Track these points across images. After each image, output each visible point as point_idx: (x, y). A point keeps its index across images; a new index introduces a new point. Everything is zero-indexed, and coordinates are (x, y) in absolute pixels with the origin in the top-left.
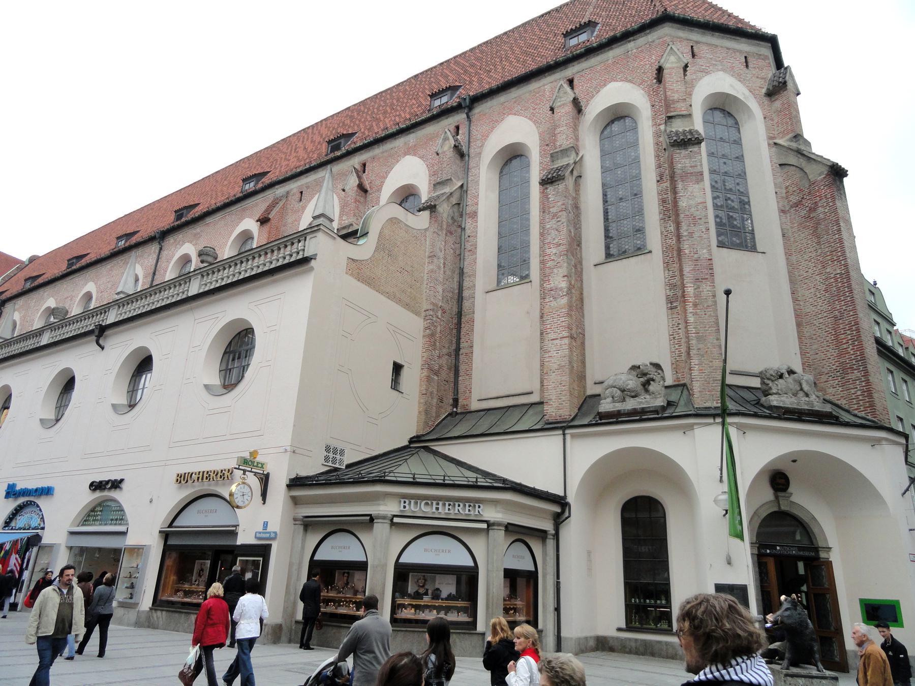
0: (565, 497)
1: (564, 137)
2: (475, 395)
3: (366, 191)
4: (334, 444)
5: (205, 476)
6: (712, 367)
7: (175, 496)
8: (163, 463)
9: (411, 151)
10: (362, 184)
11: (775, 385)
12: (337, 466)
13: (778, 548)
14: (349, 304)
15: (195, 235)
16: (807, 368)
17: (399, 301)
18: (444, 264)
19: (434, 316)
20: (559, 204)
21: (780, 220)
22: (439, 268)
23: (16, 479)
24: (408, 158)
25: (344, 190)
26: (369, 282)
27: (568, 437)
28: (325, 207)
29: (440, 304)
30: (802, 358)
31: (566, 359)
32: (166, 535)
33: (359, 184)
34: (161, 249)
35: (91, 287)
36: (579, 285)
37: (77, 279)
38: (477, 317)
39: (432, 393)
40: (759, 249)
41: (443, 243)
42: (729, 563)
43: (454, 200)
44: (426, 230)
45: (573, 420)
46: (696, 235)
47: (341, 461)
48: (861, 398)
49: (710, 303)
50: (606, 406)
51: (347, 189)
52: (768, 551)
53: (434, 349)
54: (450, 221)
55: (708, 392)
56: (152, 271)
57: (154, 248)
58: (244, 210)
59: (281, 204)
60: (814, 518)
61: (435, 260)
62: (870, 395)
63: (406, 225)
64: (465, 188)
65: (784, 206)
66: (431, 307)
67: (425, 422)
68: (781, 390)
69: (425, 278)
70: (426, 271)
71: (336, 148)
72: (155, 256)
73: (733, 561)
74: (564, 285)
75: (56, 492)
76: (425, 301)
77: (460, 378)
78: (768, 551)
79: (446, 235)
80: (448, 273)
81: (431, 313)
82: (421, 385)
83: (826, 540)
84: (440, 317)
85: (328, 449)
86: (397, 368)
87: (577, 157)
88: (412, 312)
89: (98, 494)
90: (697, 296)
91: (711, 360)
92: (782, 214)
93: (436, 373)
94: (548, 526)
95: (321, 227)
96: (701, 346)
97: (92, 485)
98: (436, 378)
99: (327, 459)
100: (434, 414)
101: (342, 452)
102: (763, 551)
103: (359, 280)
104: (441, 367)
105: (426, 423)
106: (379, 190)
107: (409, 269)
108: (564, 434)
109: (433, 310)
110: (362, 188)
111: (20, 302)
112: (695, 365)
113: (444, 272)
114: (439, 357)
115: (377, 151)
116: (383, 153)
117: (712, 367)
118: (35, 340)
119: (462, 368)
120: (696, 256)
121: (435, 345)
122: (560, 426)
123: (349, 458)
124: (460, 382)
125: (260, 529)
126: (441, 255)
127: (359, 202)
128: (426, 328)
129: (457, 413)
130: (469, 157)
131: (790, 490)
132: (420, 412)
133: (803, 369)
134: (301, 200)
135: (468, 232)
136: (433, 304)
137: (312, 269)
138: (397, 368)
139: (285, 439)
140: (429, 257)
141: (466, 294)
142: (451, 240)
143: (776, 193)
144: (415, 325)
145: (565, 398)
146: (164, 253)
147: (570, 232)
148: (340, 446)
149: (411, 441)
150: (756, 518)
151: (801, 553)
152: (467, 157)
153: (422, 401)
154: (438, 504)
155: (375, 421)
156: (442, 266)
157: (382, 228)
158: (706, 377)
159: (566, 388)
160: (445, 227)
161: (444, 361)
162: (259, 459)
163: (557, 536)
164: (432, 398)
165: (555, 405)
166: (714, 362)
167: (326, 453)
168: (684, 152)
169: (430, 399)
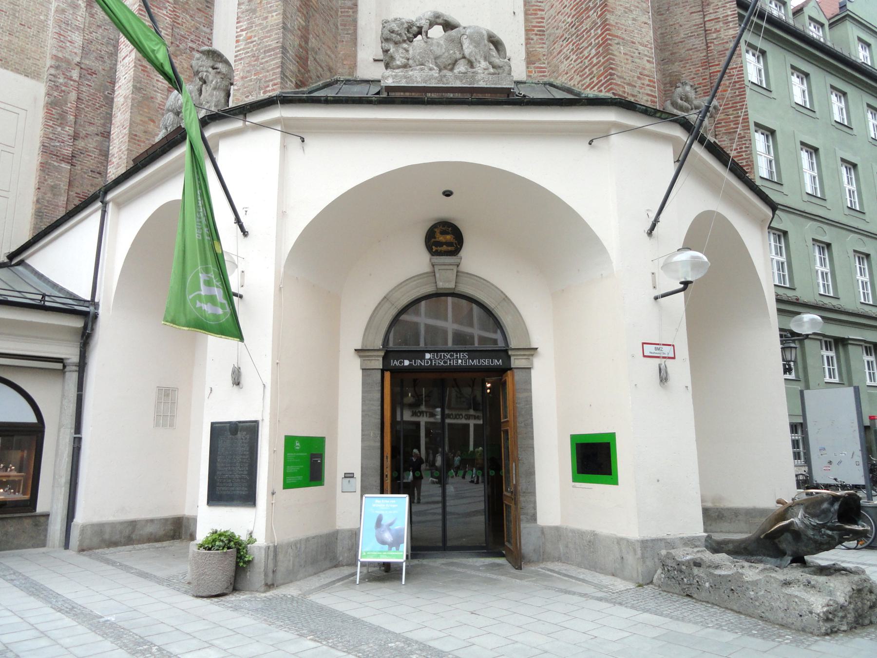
0: (93, 302)
6: (267, 27)
11: (401, 50)
13: (428, 356)
16: (535, 38)
19: (62, 76)
27: (110, 208)
29: (78, 59)
30: (526, 20)
39: (53, 188)
42: (237, 383)
48: (595, 61)
52: (407, 363)
55: (255, 74)
60: (506, 299)
62: (607, 51)
66: (53, 63)
68: (413, 58)
69: (51, 23)
73: (244, 380)
78: (407, 363)
81: (53, 71)
83: (526, 333)
91: (265, 15)
93: (72, 160)
94: (70, 353)
98: (66, 166)
102: (396, 363)
112: (242, 31)
114: (75, 137)
117: (267, 27)
121: (62, 117)
128: (48, 94)
131: (463, 253)
133: (528, 40)
136: (56, 58)
150: (387, 305)
151: (476, 362)
153: (35, 199)
158: (254, 49)
159: (126, 131)
163: (82, 366)
164: (54, 195)
166: (270, 18)
169: (49, 195)
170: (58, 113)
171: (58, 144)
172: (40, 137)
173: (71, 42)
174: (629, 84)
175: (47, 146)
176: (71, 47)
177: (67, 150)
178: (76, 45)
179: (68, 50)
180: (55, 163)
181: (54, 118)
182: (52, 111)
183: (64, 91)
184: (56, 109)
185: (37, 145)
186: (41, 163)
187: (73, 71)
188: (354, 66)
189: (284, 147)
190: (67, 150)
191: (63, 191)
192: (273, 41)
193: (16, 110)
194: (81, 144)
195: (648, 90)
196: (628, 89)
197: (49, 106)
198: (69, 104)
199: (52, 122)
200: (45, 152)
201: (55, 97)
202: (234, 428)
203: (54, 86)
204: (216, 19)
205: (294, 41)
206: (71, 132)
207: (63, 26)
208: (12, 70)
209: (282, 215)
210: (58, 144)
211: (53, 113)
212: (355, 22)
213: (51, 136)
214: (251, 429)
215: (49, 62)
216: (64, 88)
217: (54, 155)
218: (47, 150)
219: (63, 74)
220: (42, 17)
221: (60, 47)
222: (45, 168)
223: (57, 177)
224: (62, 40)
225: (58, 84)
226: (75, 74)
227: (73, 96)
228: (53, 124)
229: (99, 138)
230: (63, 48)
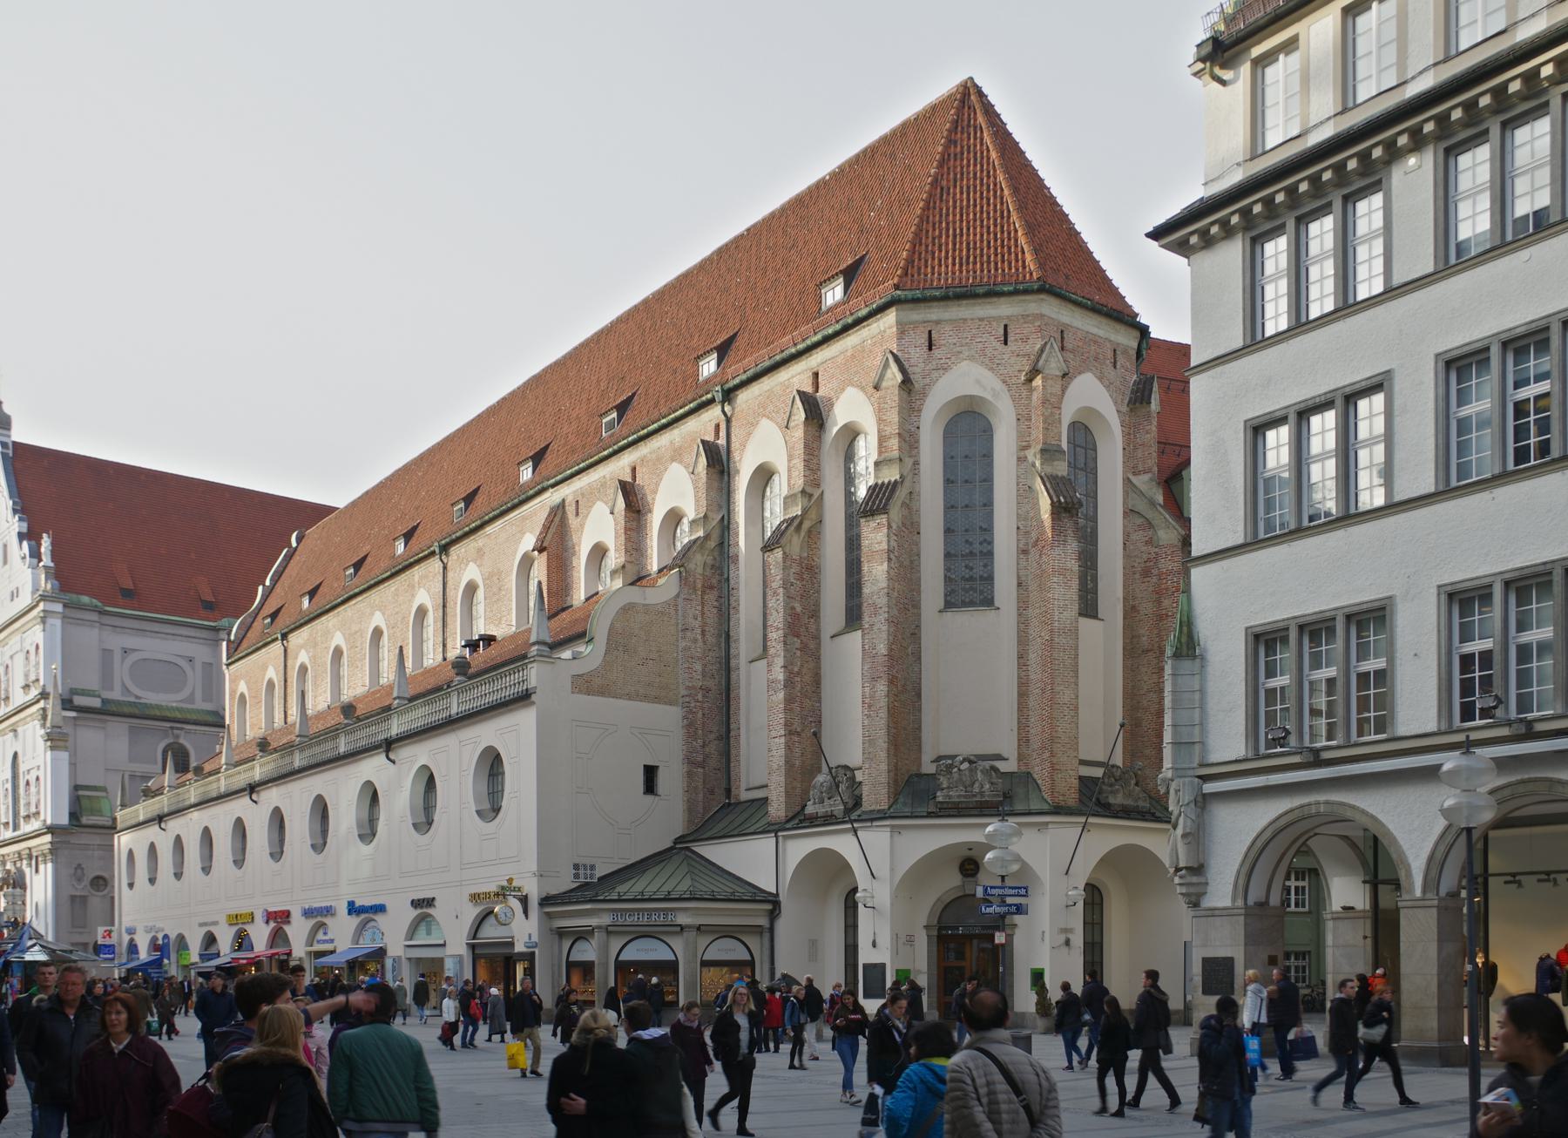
1: (797, 473)
2: (743, 786)
3: (639, 512)
5: (487, 895)
7: (472, 912)
14: (578, 723)
15: (479, 550)
17: (646, 698)
18: (703, 633)
20: (778, 578)
21: (1018, 564)
22: (695, 641)
26: (603, 691)
27: (780, 839)
28: (538, 634)
31: (783, 759)
32: (473, 947)
36: (812, 665)
38: (743, 693)
40: (997, 603)
43: (712, 544)
44: (678, 596)
45: (788, 821)
46: (875, 628)
47: (592, 876)
49: (882, 704)
50: (810, 809)
51: (615, 512)
53: (696, 740)
54: (708, 572)
57: (434, 565)
58: (524, 519)
59: (557, 519)
61: (689, 634)
63: (644, 605)
64: (726, 522)
65: (1027, 544)
74: (781, 677)
77: (732, 765)
79: (703, 593)
80: (711, 639)
81: (687, 699)
84: (700, 700)
87: (810, 500)
88: (666, 703)
90: (872, 697)
92: (1021, 556)
93: (702, 765)
96: (871, 750)
100: (701, 811)
104: (706, 756)
108: (776, 836)
113: (704, 642)
114: (703, 747)
118: (329, 745)
119: (733, 752)
120: (874, 652)
122: (775, 829)
124: (732, 769)
126: (697, 624)
127: (630, 529)
128: (685, 717)
129: (729, 804)
130: (729, 475)
134: (577, 514)
135: (732, 582)
136: (688, 688)
141: (733, 663)
142: (711, 597)
143: (1018, 528)
144: (669, 718)
145: (782, 799)
146: (450, 575)
147: (793, 608)
152: (726, 477)
155: (627, 832)
156: (699, 637)
159: (783, 789)
160: (699, 586)
161: (713, 748)
165: (776, 806)
168: (873, 524)
174: (1063, 795)
188: (920, 765)
189: (891, 836)
192: (884, 778)
193: (668, 734)
194: (707, 749)
195: (1073, 796)
196: (1061, 798)
202: (875, 965)
203: (691, 712)
204: (823, 695)
205: (892, 774)
209: (892, 870)
212: (920, 738)
214: (883, 965)
218: (689, 761)
222: (690, 774)
226: (700, 697)
227: (700, 715)
229: (716, 742)
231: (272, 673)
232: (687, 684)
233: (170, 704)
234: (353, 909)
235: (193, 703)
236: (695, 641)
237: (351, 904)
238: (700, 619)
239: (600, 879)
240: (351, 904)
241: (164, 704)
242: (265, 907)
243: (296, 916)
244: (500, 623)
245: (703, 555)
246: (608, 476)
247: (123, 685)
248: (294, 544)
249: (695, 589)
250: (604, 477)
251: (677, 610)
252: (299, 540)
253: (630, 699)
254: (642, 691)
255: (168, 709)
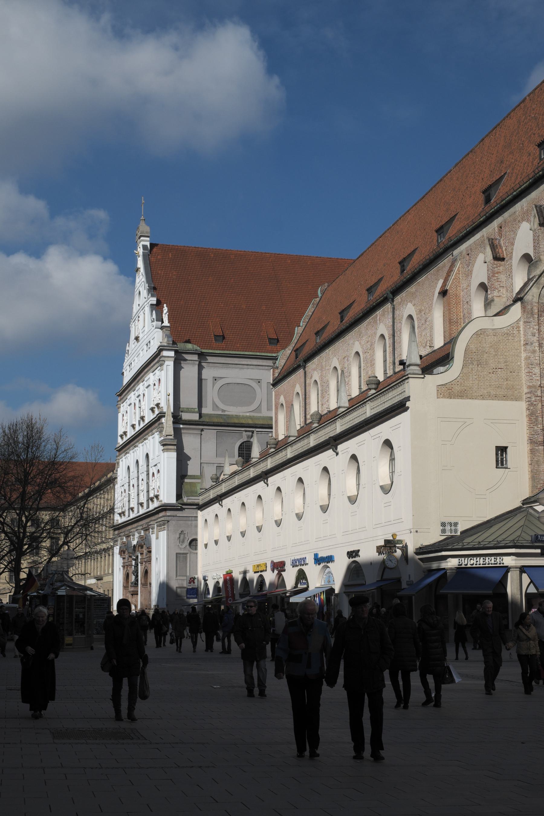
4: (446, 520)
8: (371, 539)
9: (525, 217)
10: (496, 257)
12: (453, 534)
17: (496, 397)
23: (319, 550)
24: (524, 222)
25: (486, 262)
26: (461, 395)
33: (493, 257)
34: (394, 309)
35: (357, 347)
37: (350, 337)
41: (537, 327)
51: (487, 261)
56: (391, 332)
61: (528, 347)
63: (493, 329)
67: (532, 486)
69: (523, 365)
70: (523, 359)
71: (488, 200)
72: (391, 315)
75: (335, 559)
76: (524, 385)
81: (529, 395)
82: (528, 457)
85: (443, 524)
86: (502, 450)
88: (512, 400)
89: (352, 560)
95: (409, 376)
97: (348, 553)
99: (444, 531)
101: (456, 524)
103: (451, 398)
105: (533, 487)
106: (511, 258)
107: (502, 365)
109: (530, 393)
110: (498, 258)
111: (316, 360)
115: (506, 215)
116: (510, 216)
121: (536, 420)
123: (461, 528)
125: (408, 580)
126: (535, 339)
127: (498, 273)
128: (528, 409)
132: (529, 478)
136: (529, 387)
137: (408, 408)
138: (502, 450)
139: (408, 524)
140: (524, 345)
146: (397, 312)
148: (453, 521)
149: (525, 502)
153: (530, 470)
154: (477, 559)
156: (537, 348)
157: (467, 345)
160: (536, 311)
162: (398, 538)
164: (538, 466)
167: (442, 528)
169: (536, 466)
170: (535, 419)
171: (536, 436)
172: (527, 433)
173: (534, 374)
175: (532, 439)
176: (535, 377)
177: (541, 438)
178: (537, 375)
179: (534, 379)
180: (537, 448)
181: (533, 422)
182: (531, 418)
183: (535, 405)
184: (533, 417)
185: (526, 438)
186: (530, 450)
187: (538, 391)
190: (541, 438)
191: (542, 462)
197: (530, 416)
198: (539, 411)
199: (532, 425)
200: (532, 443)
201: (532, 410)
203: (532, 404)
206: (542, 428)
207: (530, 366)
208: (510, 400)
210: (536, 436)
211: (532, 419)
213: (533, 433)
215: (526, 390)
216: (535, 403)
217: (535, 443)
219: (534, 395)
220: (519, 363)
221: (530, 379)
223: (538, 455)
224: (531, 375)
225: (532, 402)
226: (539, 394)
228: (533, 426)
230: (531, 379)
231: (298, 389)
232: (528, 384)
233: (245, 414)
234: (318, 560)
235: (260, 412)
236: (534, 352)
237: (316, 555)
238: (537, 335)
239: (462, 533)
240: (316, 555)
241: (241, 414)
242: (272, 559)
243: (288, 566)
244: (426, 345)
245: (538, 288)
246: (485, 235)
247: (214, 403)
248: (320, 295)
249: (532, 314)
250: (483, 236)
251: (519, 331)
252: (323, 294)
253: (483, 399)
254: (493, 392)
255: (243, 417)
